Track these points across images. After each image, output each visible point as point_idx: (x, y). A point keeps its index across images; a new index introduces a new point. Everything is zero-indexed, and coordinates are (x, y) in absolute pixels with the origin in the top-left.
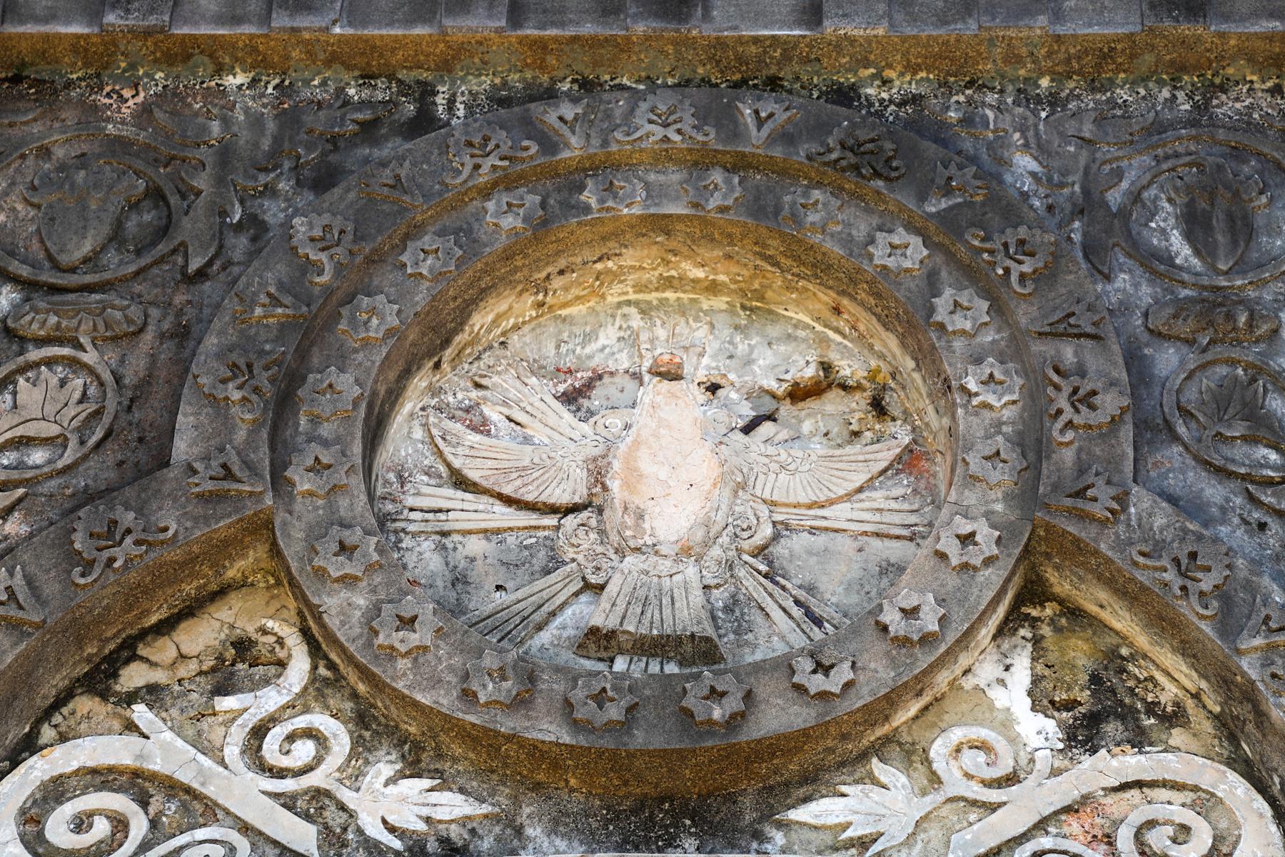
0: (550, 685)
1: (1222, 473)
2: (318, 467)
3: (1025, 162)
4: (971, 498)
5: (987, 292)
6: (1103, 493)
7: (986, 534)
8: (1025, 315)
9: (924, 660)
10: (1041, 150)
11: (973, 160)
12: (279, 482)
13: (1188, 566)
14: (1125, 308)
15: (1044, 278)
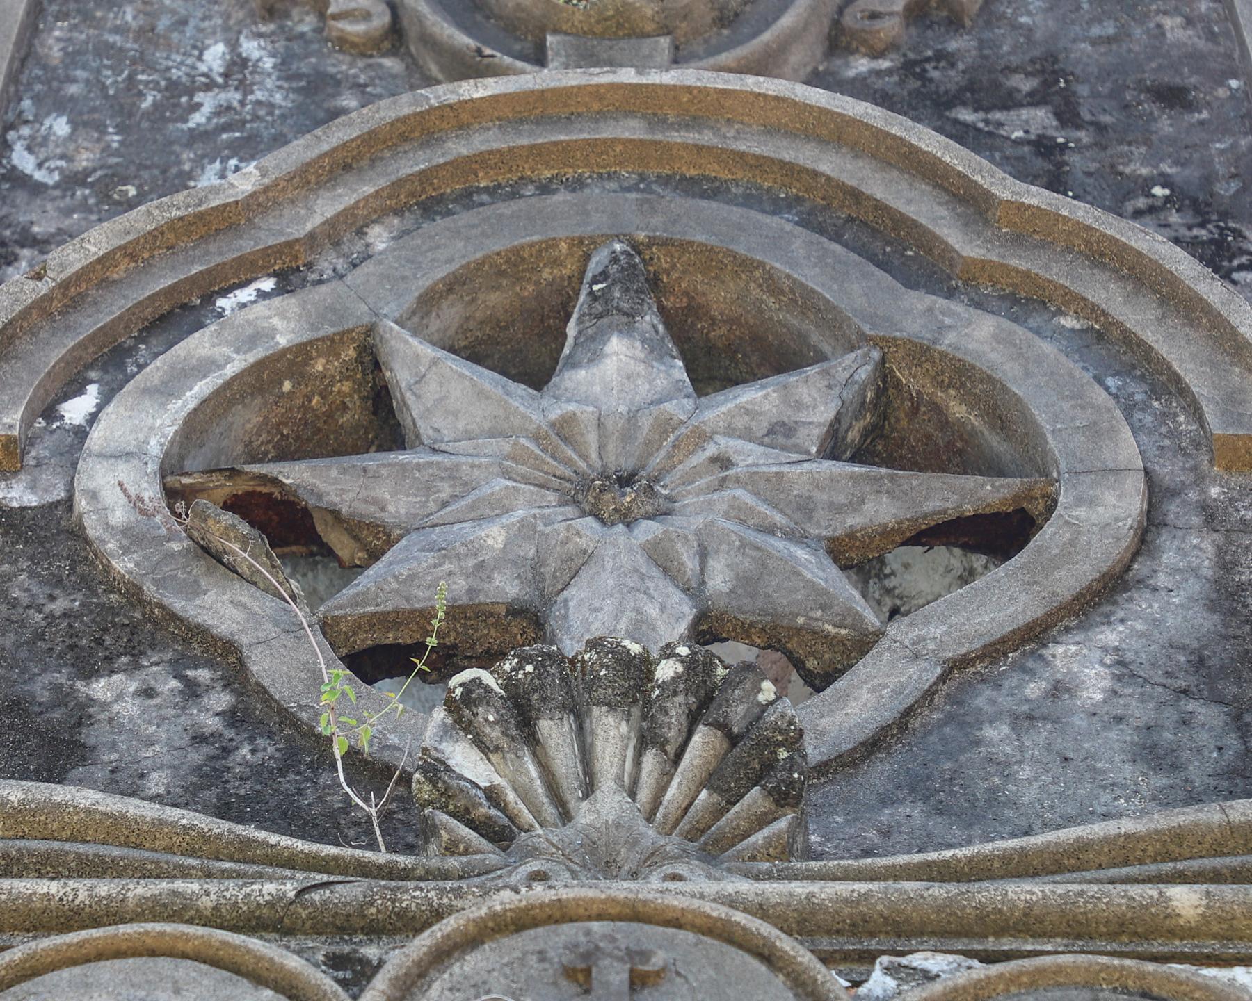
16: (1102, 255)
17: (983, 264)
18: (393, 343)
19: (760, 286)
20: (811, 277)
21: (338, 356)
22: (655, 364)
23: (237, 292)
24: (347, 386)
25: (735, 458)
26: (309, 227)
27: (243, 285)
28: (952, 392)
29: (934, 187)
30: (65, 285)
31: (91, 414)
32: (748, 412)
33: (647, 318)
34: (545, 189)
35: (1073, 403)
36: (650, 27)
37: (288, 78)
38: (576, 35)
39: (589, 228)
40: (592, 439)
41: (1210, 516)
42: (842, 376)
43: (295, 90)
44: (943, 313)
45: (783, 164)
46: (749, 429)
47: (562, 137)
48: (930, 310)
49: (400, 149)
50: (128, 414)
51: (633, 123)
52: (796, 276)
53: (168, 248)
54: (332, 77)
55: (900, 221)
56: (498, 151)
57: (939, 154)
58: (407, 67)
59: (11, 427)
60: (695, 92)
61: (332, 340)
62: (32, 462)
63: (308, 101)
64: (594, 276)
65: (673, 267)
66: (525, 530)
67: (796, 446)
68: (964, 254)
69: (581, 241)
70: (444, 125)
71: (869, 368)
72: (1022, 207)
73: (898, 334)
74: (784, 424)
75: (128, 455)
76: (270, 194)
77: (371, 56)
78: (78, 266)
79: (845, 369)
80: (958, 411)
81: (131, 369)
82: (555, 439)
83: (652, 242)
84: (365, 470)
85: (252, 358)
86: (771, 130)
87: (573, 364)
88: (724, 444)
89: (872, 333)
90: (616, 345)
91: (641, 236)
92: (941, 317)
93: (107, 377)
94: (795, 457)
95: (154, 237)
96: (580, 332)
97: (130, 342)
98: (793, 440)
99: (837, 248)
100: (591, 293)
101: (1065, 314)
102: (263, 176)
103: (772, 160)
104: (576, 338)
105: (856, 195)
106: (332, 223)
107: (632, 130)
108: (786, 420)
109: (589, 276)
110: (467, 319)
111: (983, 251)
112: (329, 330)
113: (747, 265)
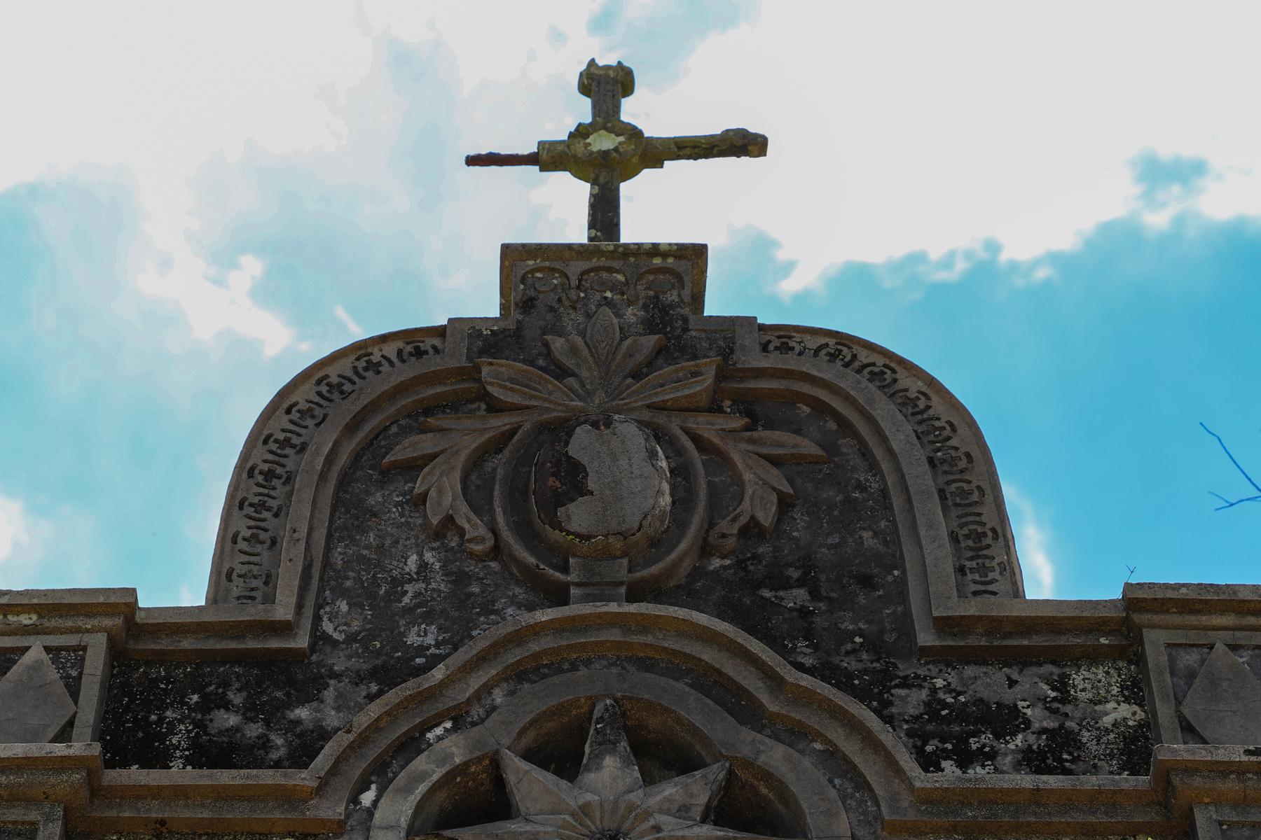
16: (835, 712)
17: (778, 715)
18: (507, 760)
19: (673, 720)
20: (697, 720)
21: (481, 764)
22: (626, 770)
23: (435, 729)
24: (484, 776)
25: (663, 827)
26: (467, 695)
27: (437, 725)
28: (762, 783)
29: (757, 669)
30: (360, 734)
31: (373, 801)
32: (669, 800)
33: (622, 744)
34: (574, 667)
35: (819, 797)
36: (618, 553)
37: (446, 575)
38: (584, 557)
39: (595, 691)
40: (598, 814)
42: (712, 778)
43: (450, 582)
44: (759, 743)
45: (685, 654)
46: (669, 809)
47: (582, 640)
48: (753, 741)
49: (508, 647)
50: (391, 803)
51: (615, 631)
52: (691, 719)
53: (405, 708)
54: (467, 573)
55: (740, 687)
56: (554, 648)
57: (760, 655)
58: (502, 567)
59: (341, 814)
60: (645, 616)
61: (479, 758)
62: (349, 828)
63: (456, 588)
64: (597, 719)
65: (633, 708)
67: (690, 817)
68: (770, 710)
69: (591, 697)
70: (528, 633)
71: (724, 772)
72: (799, 686)
73: (738, 755)
74: (685, 806)
75: (390, 827)
76: (450, 678)
77: (485, 561)
78: (366, 725)
79: (713, 774)
80: (764, 791)
81: (390, 775)
82: (581, 814)
83: (624, 698)
84: (497, 836)
85: (444, 770)
86: (681, 634)
87: (589, 770)
88: (661, 819)
89: (726, 754)
90: (610, 762)
91: (619, 695)
92: (758, 745)
93: (380, 780)
94: (690, 823)
95: (398, 706)
96: (591, 752)
97: (389, 759)
98: (689, 814)
99: (710, 702)
100: (596, 729)
101: (816, 741)
102: (447, 669)
103: (680, 652)
104: (589, 754)
105: (719, 672)
106: (477, 691)
107: (614, 635)
108: (686, 804)
109: (594, 720)
110: (538, 735)
111: (779, 708)
112: (478, 754)
113: (667, 710)
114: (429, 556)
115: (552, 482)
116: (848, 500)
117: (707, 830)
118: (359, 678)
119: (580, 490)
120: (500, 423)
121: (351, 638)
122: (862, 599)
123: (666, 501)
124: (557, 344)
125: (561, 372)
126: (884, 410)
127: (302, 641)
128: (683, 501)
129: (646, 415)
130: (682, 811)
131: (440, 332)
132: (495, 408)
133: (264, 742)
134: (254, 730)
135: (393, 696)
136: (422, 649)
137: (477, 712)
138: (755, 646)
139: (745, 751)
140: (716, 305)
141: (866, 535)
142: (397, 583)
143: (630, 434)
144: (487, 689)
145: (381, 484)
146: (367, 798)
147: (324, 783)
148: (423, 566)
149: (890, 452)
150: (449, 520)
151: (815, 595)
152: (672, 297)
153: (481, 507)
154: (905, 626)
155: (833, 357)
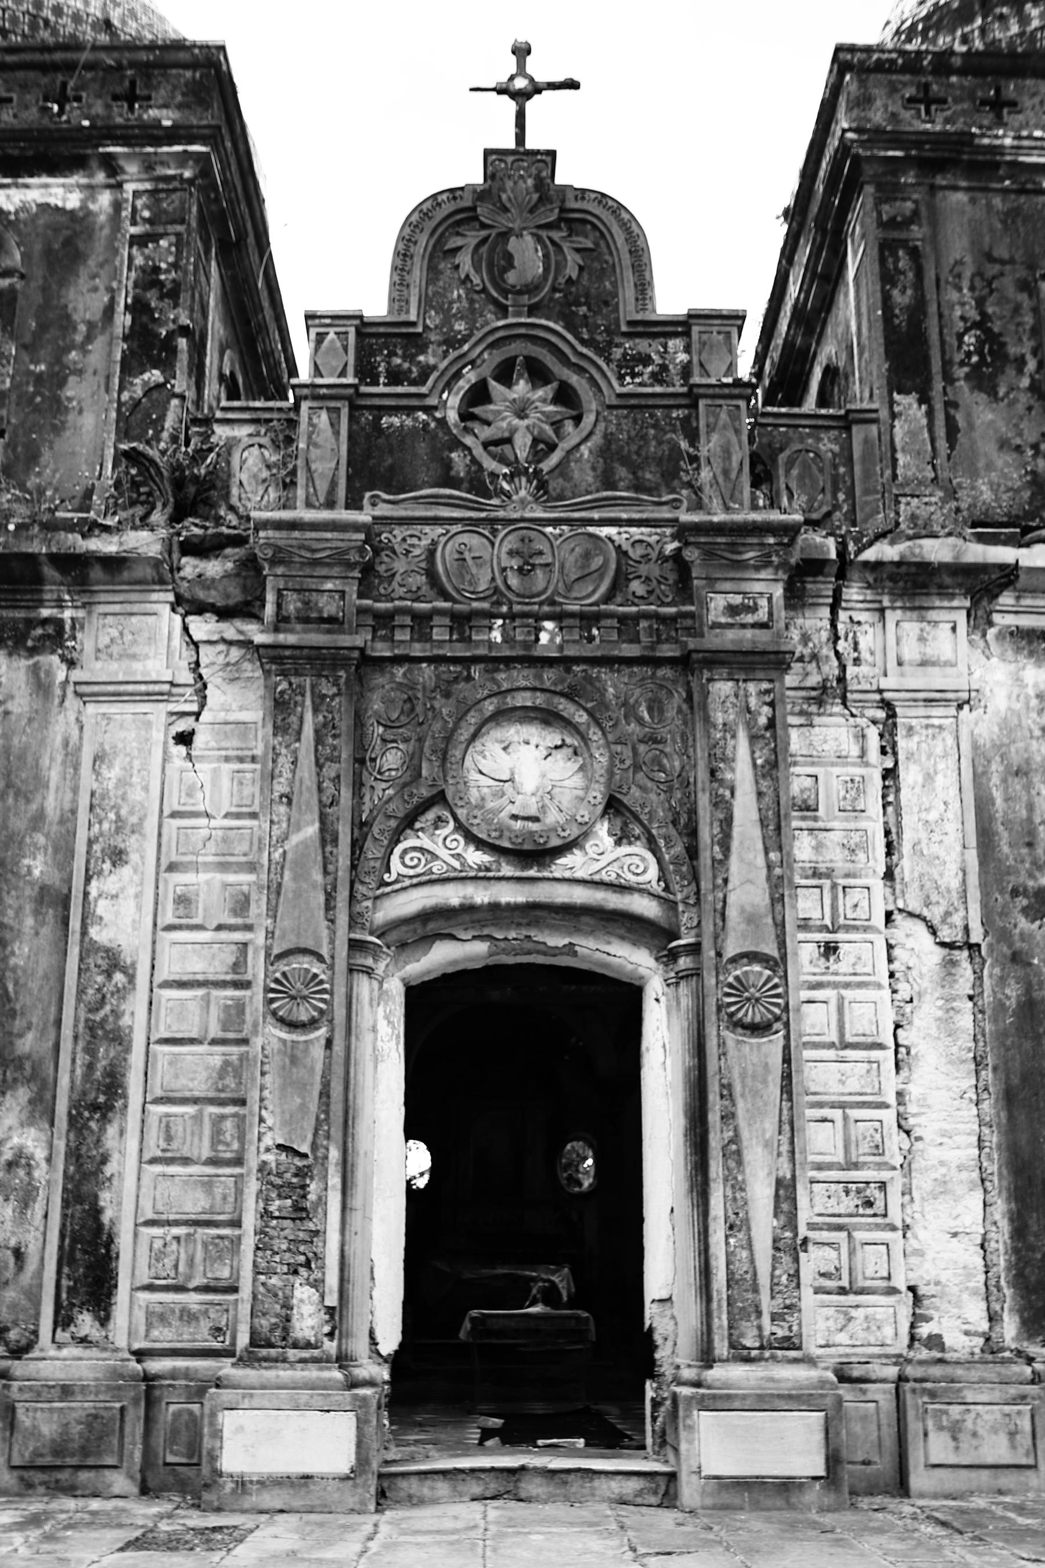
0: (506, 834)
1: (652, 780)
2: (454, 777)
3: (611, 690)
4: (596, 786)
5: (602, 729)
6: (625, 787)
7: (599, 796)
8: (610, 737)
9: (585, 828)
10: (615, 687)
11: (598, 689)
12: (446, 781)
13: (643, 806)
14: (633, 733)
15: (614, 726)
20: (550, 365)
41: (605, 419)
66: (509, 424)
88: (538, 404)
90: (522, 382)
114: (461, 291)
115: (503, 263)
116: (602, 269)
117: (551, 408)
118: (440, 344)
119: (511, 266)
120: (484, 233)
121: (436, 327)
122: (604, 311)
123: (541, 270)
124: (504, 197)
125: (506, 210)
126: (616, 229)
127: (420, 329)
128: (546, 269)
129: (534, 231)
130: (544, 401)
131: (462, 189)
132: (484, 226)
133: (410, 371)
134: (406, 365)
135: (453, 354)
136: (460, 332)
137: (479, 362)
138: (569, 337)
139: (564, 378)
140: (559, 180)
141: (607, 283)
142: (451, 303)
143: (528, 239)
144: (482, 353)
145: (444, 258)
146: (445, 396)
147: (431, 391)
148: (459, 296)
149: (617, 249)
150: (467, 276)
151: (589, 309)
152: (544, 174)
153: (477, 269)
154: (618, 319)
155: (600, 202)
